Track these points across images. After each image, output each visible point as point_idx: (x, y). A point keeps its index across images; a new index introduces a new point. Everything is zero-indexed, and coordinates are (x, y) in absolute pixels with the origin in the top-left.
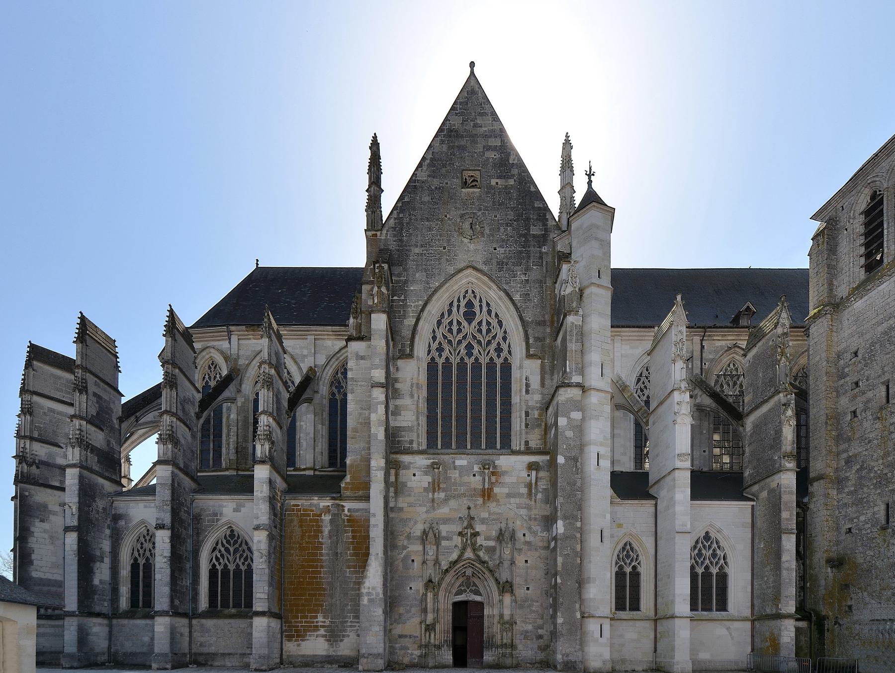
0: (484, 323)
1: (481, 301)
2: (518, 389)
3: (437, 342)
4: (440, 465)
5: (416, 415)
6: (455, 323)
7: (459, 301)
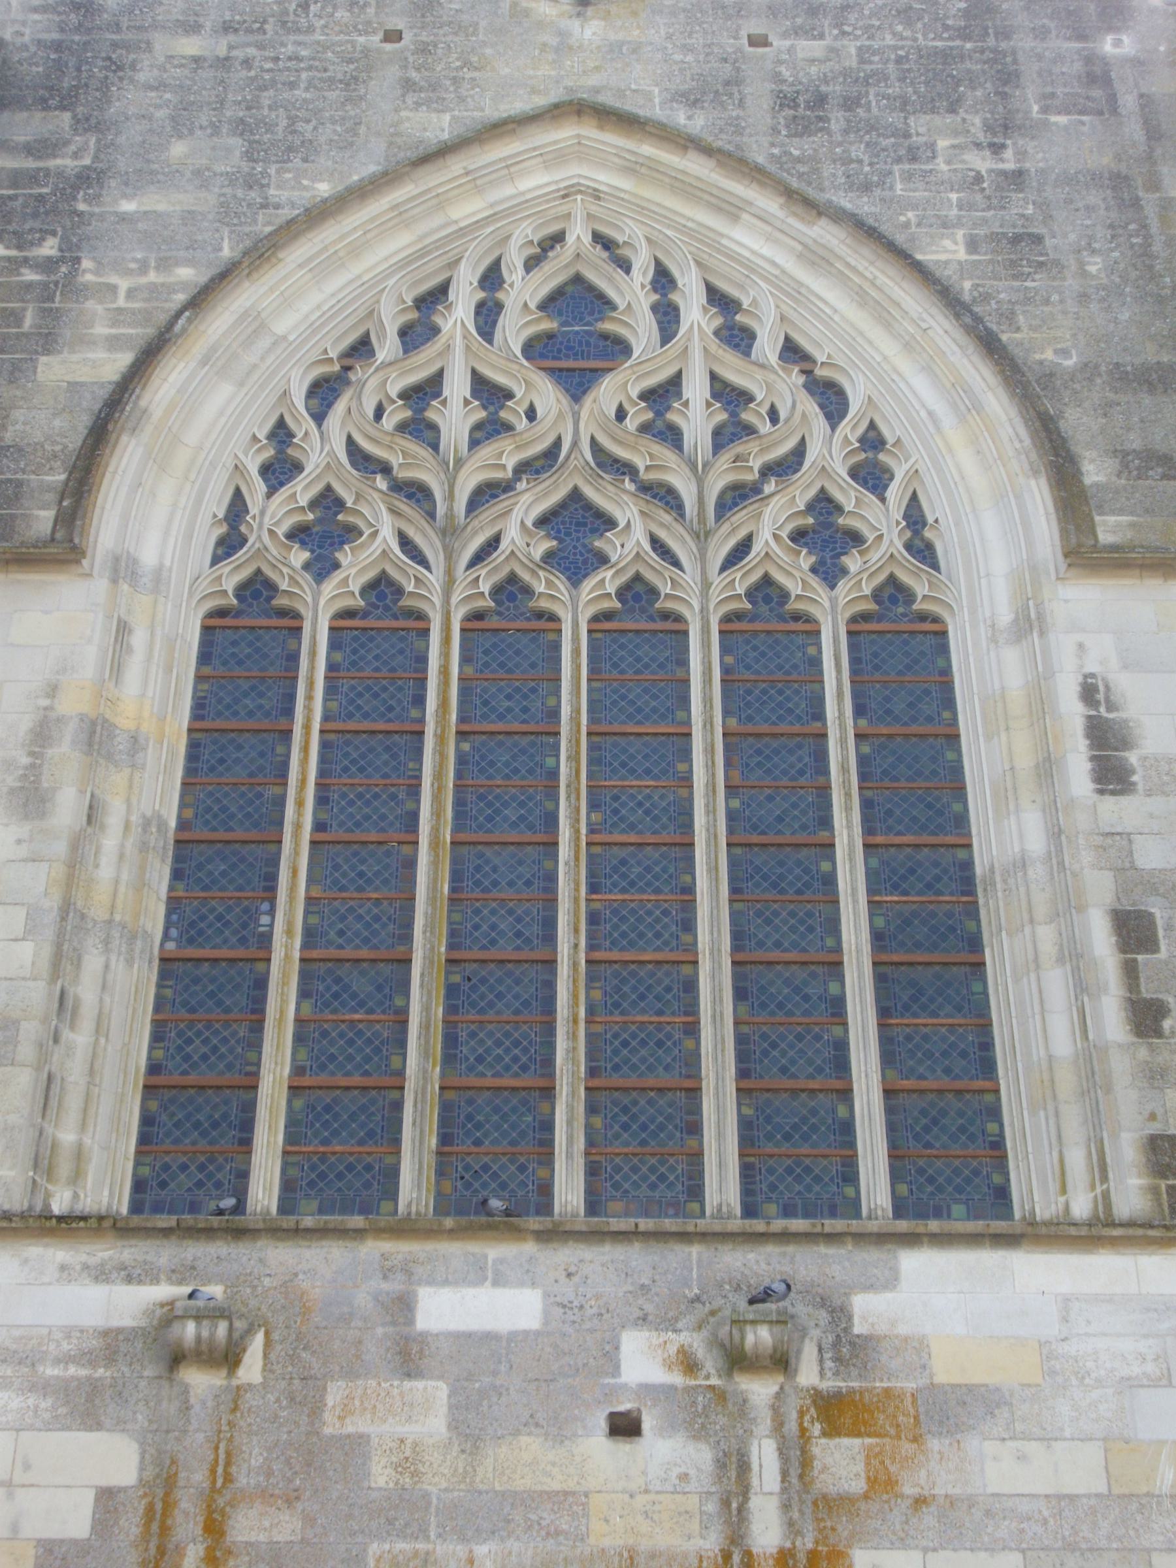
0: (696, 389)
1: (663, 279)
2: (1025, 761)
3: (302, 490)
4: (250, 1331)
5: (49, 933)
6: (457, 386)
7: (492, 278)
